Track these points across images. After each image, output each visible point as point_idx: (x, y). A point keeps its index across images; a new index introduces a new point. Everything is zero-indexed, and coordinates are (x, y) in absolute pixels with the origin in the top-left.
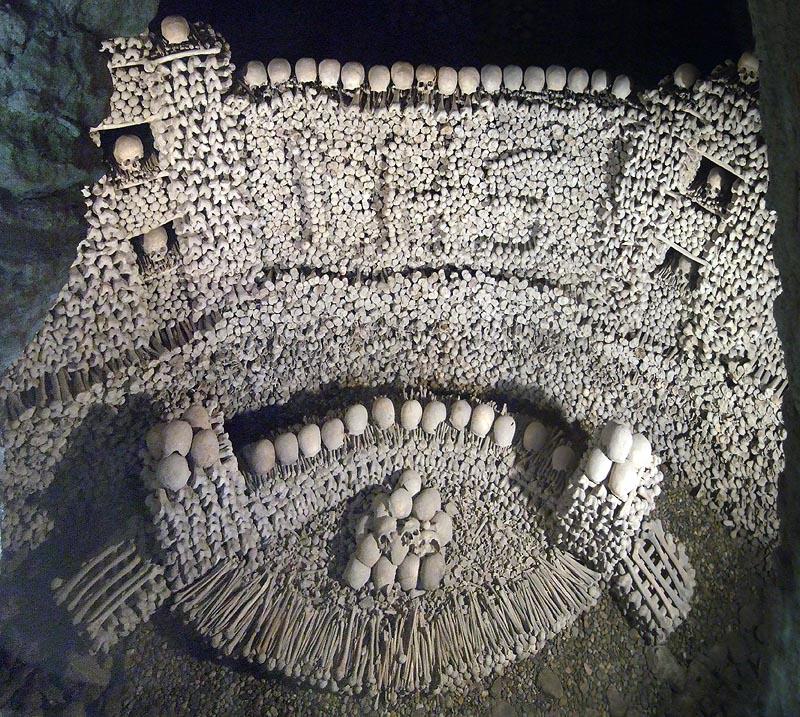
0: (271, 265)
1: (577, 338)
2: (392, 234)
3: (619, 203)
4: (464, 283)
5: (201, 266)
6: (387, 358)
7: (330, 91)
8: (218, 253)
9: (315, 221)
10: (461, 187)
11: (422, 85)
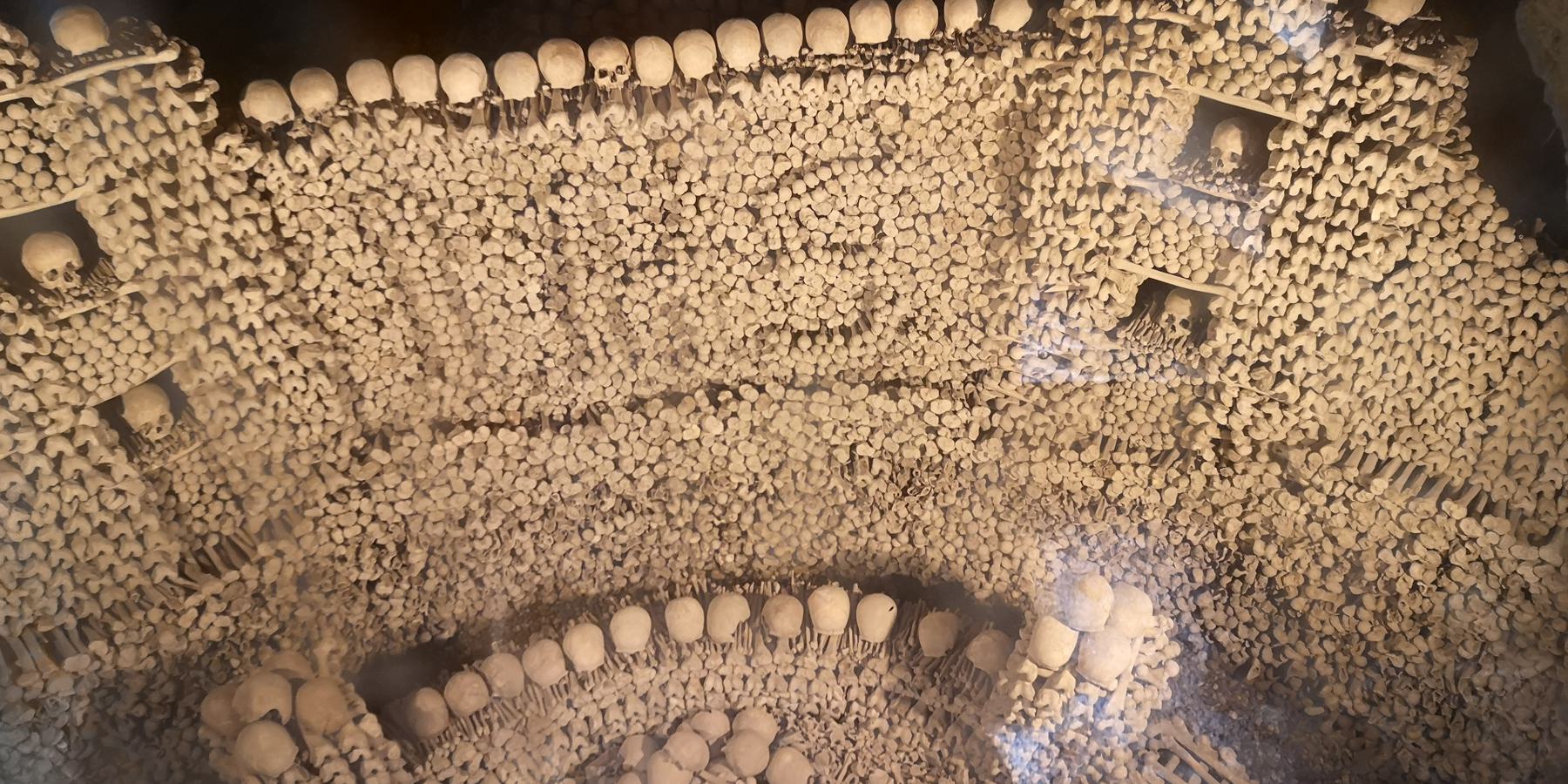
0: (375, 426)
1: (975, 465)
2: (594, 343)
3: (1030, 220)
5: (242, 437)
6: (623, 545)
8: (269, 413)
10: (713, 246)
11: (603, 74)
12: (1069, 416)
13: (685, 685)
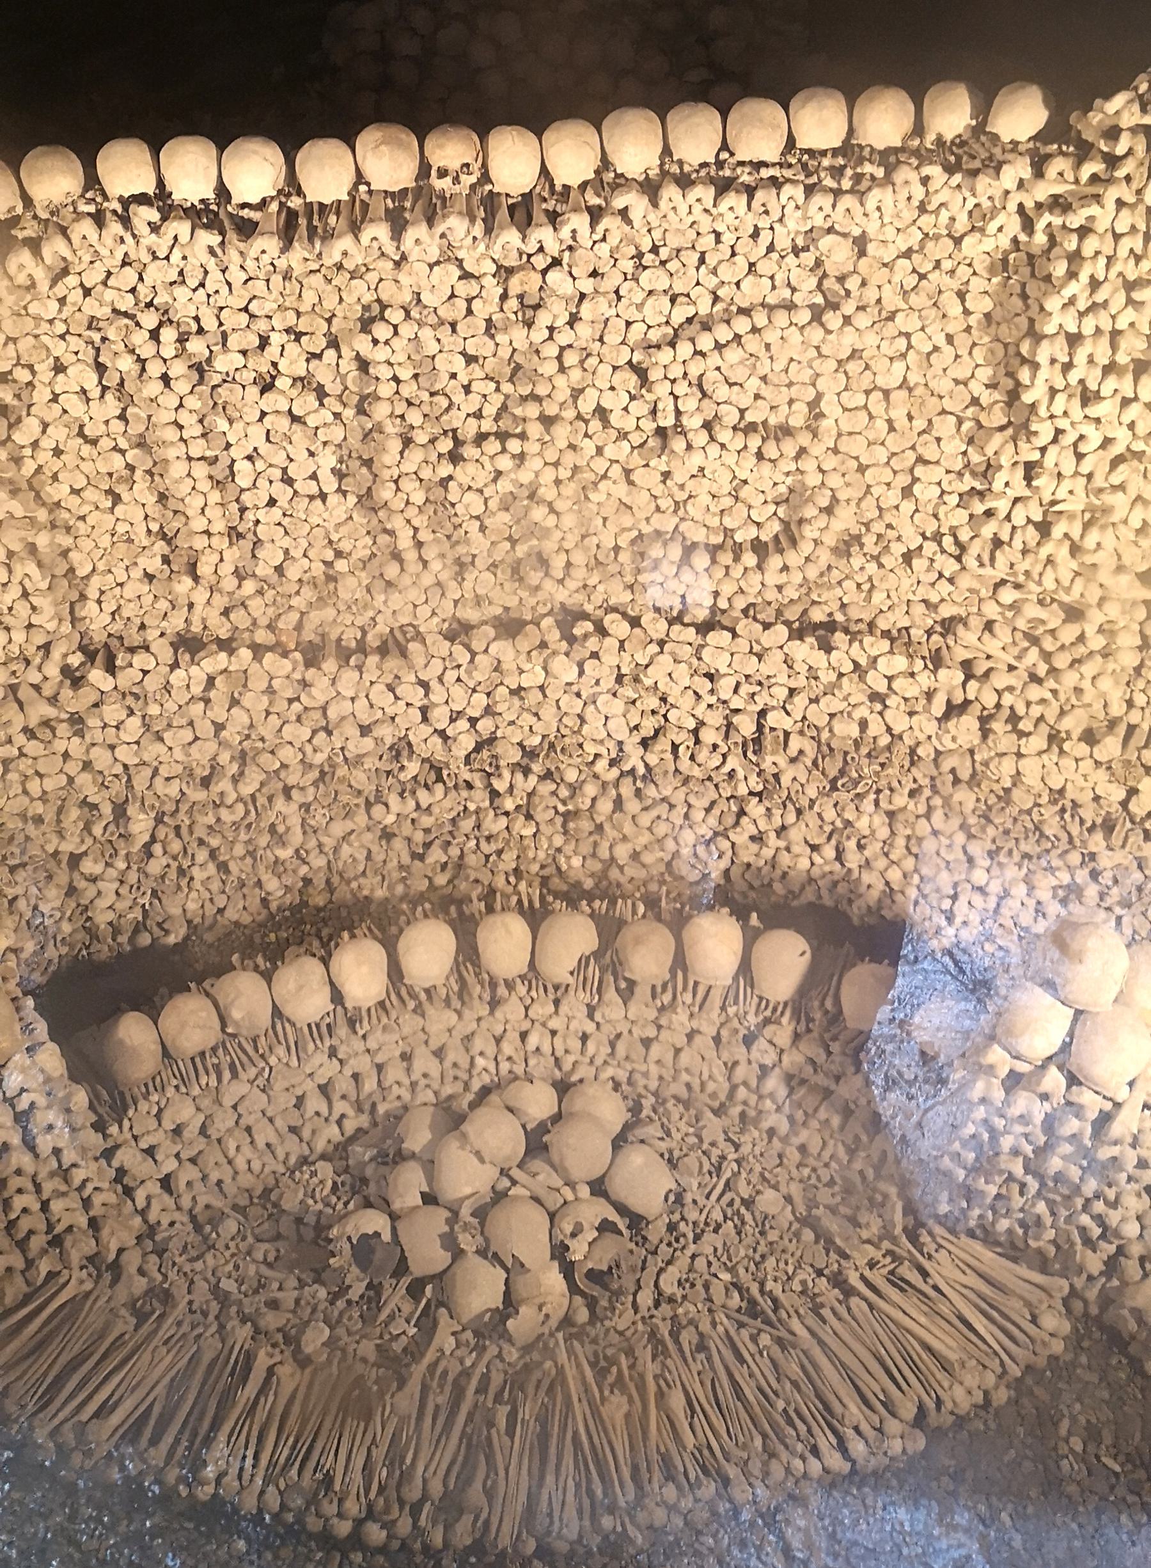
0: (99, 637)
1: (938, 753)
2: (405, 541)
3: (1033, 406)
4: (611, 643)
6: (427, 831)
7: (198, 213)
9: (199, 524)
10: (579, 417)
11: (443, 173)
12: (1078, 691)
13: (498, 1040)
